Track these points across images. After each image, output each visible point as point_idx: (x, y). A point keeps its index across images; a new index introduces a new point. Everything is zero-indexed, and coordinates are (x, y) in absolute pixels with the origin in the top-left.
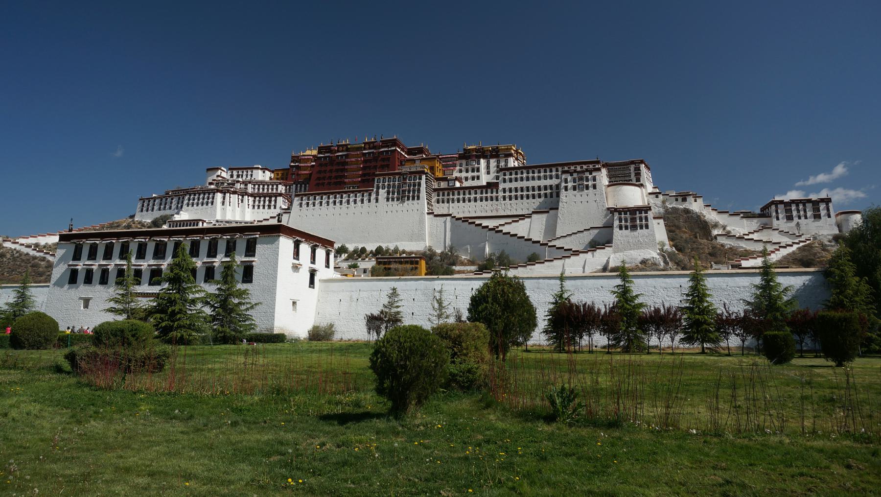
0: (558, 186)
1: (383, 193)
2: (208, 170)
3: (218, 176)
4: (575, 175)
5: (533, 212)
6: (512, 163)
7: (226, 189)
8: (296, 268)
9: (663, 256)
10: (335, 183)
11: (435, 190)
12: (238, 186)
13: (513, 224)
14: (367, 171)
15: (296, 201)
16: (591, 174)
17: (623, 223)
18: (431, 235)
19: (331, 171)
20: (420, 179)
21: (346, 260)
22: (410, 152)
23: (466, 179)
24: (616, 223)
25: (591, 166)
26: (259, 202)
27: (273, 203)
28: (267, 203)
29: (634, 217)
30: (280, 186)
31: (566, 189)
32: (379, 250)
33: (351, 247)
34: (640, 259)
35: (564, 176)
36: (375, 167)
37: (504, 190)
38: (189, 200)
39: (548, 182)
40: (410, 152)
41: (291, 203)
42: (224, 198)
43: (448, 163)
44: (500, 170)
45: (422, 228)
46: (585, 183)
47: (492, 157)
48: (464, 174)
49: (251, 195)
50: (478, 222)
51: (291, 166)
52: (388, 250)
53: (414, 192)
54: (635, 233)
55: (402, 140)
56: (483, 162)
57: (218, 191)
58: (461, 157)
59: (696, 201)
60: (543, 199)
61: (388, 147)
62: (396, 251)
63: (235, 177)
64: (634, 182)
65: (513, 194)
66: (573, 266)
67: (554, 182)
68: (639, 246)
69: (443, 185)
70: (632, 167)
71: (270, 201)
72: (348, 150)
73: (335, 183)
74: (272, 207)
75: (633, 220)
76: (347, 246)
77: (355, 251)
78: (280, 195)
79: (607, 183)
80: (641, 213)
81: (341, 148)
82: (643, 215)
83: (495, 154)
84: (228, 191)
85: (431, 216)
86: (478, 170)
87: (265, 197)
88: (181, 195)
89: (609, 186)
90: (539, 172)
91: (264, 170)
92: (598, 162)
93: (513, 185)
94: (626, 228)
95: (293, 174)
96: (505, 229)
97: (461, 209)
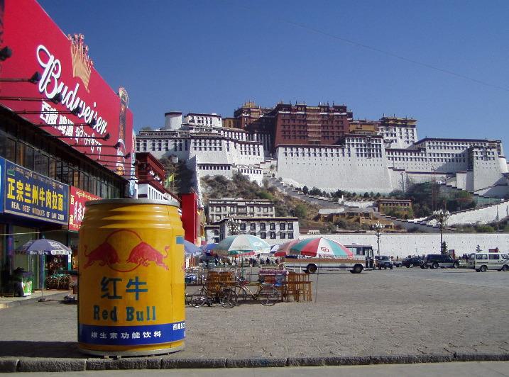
1: (353, 150)
2: (168, 114)
4: (481, 150)
27: (256, 150)
28: (252, 149)
35: (475, 150)
47: (402, 126)
53: (377, 151)
58: (383, 124)
63: (196, 122)
65: (436, 157)
72: (306, 110)
74: (257, 154)
83: (405, 123)
85: (392, 170)
86: (395, 136)
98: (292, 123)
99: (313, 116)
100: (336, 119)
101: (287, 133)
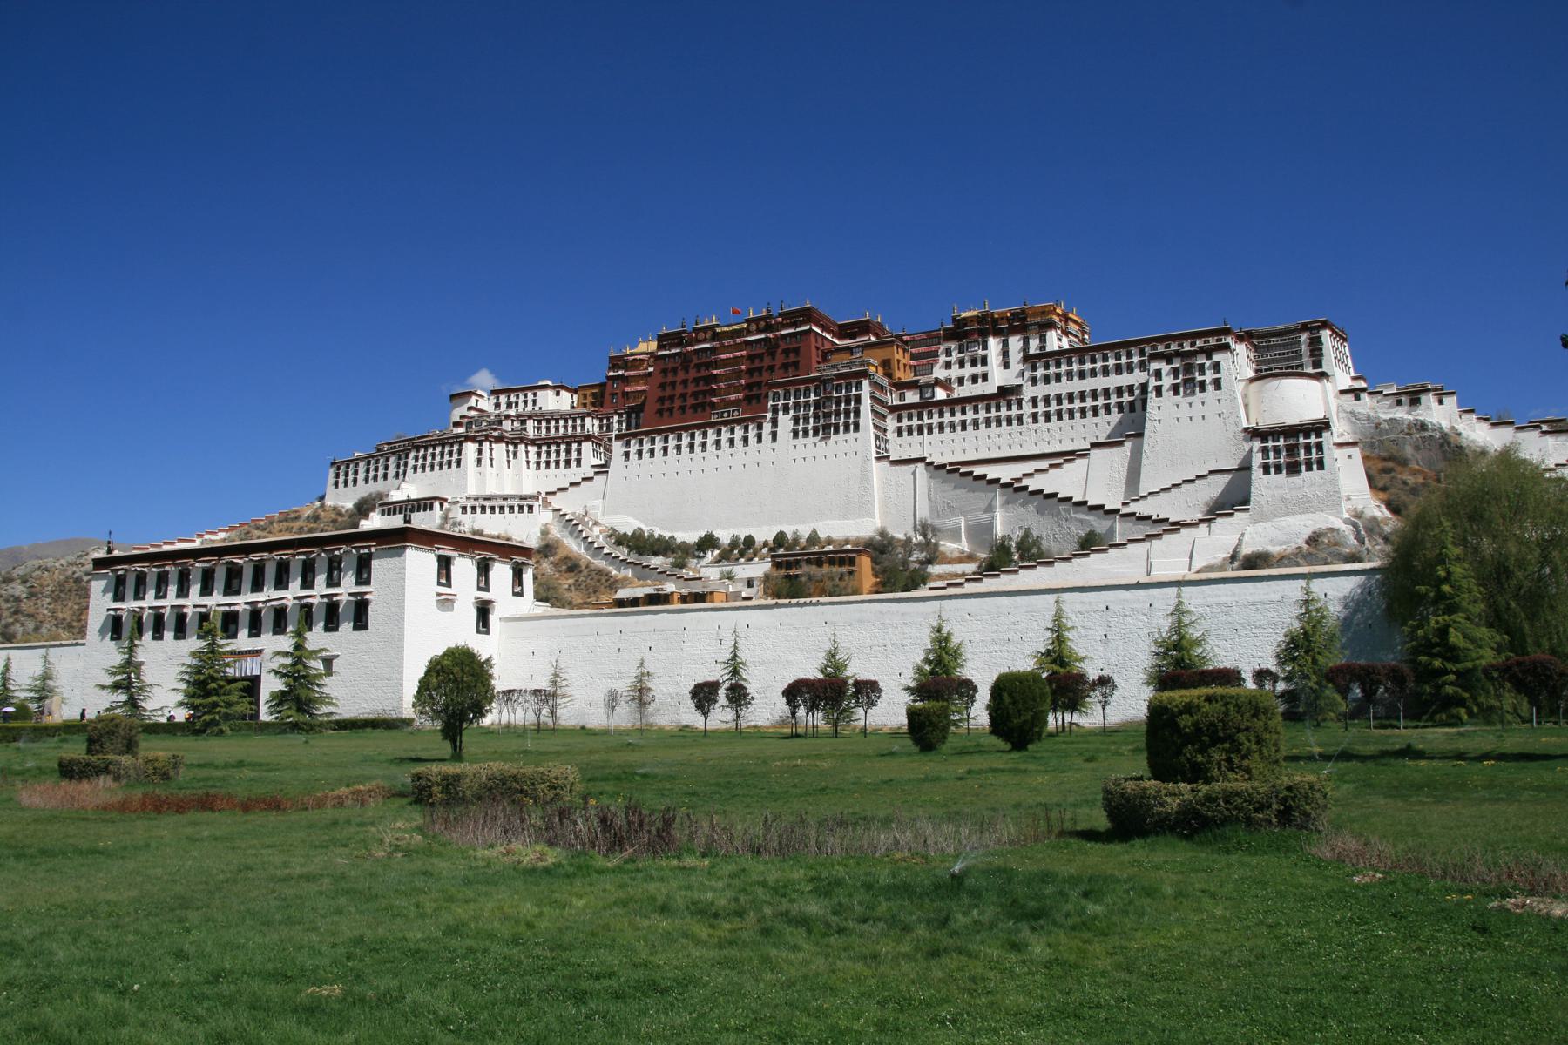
0: (1144, 387)
1: (786, 421)
3: (470, 408)
5: (1094, 445)
6: (1055, 341)
7: (484, 432)
8: (446, 603)
9: (1355, 525)
10: (695, 407)
11: (893, 409)
12: (507, 425)
13: (1051, 471)
14: (756, 378)
15: (618, 448)
16: (1209, 357)
17: (1271, 460)
18: (885, 503)
19: (685, 382)
20: (859, 386)
21: (717, 561)
22: (845, 331)
23: (961, 381)
24: (1257, 459)
25: (1213, 341)
26: (548, 453)
27: (574, 455)
28: (563, 456)
29: (1294, 446)
30: (588, 421)
31: (1159, 390)
32: (780, 539)
33: (724, 537)
34: (1306, 533)
35: (1154, 366)
36: (771, 368)
37: (1034, 401)
38: (416, 458)
39: (1125, 380)
40: (845, 331)
41: (609, 450)
42: (480, 451)
43: (925, 347)
44: (1028, 358)
45: (868, 490)
46: (1199, 378)
47: (1013, 331)
48: (955, 372)
49: (533, 442)
50: (978, 470)
51: (609, 378)
52: (796, 541)
54: (1295, 480)
55: (825, 310)
56: (994, 343)
57: (468, 438)
58: (950, 335)
59: (1441, 402)
60: (1115, 417)
61: (796, 325)
62: (813, 539)
63: (503, 407)
64: (1310, 370)
65: (1054, 407)
66: (1169, 558)
67: (1137, 378)
68: (1305, 506)
69: (912, 397)
70: (1304, 337)
71: (568, 452)
73: (695, 407)
74: (574, 463)
75: (1292, 450)
76: (717, 534)
77: (734, 544)
78: (588, 438)
79: (1252, 374)
80: (1307, 436)
81: (701, 335)
82: (1313, 439)
83: (1019, 324)
84: (487, 438)
85: (885, 464)
86: (984, 361)
87: (558, 445)
88: (404, 450)
89: (1252, 380)
90: (1105, 359)
91: (557, 389)
92: (1227, 332)
93: (1053, 389)
94: (1278, 469)
95: (613, 395)
96: (1033, 484)
97: (945, 447)
98: (681, 375)
99: (736, 347)
100: (783, 345)
101: (667, 405)
